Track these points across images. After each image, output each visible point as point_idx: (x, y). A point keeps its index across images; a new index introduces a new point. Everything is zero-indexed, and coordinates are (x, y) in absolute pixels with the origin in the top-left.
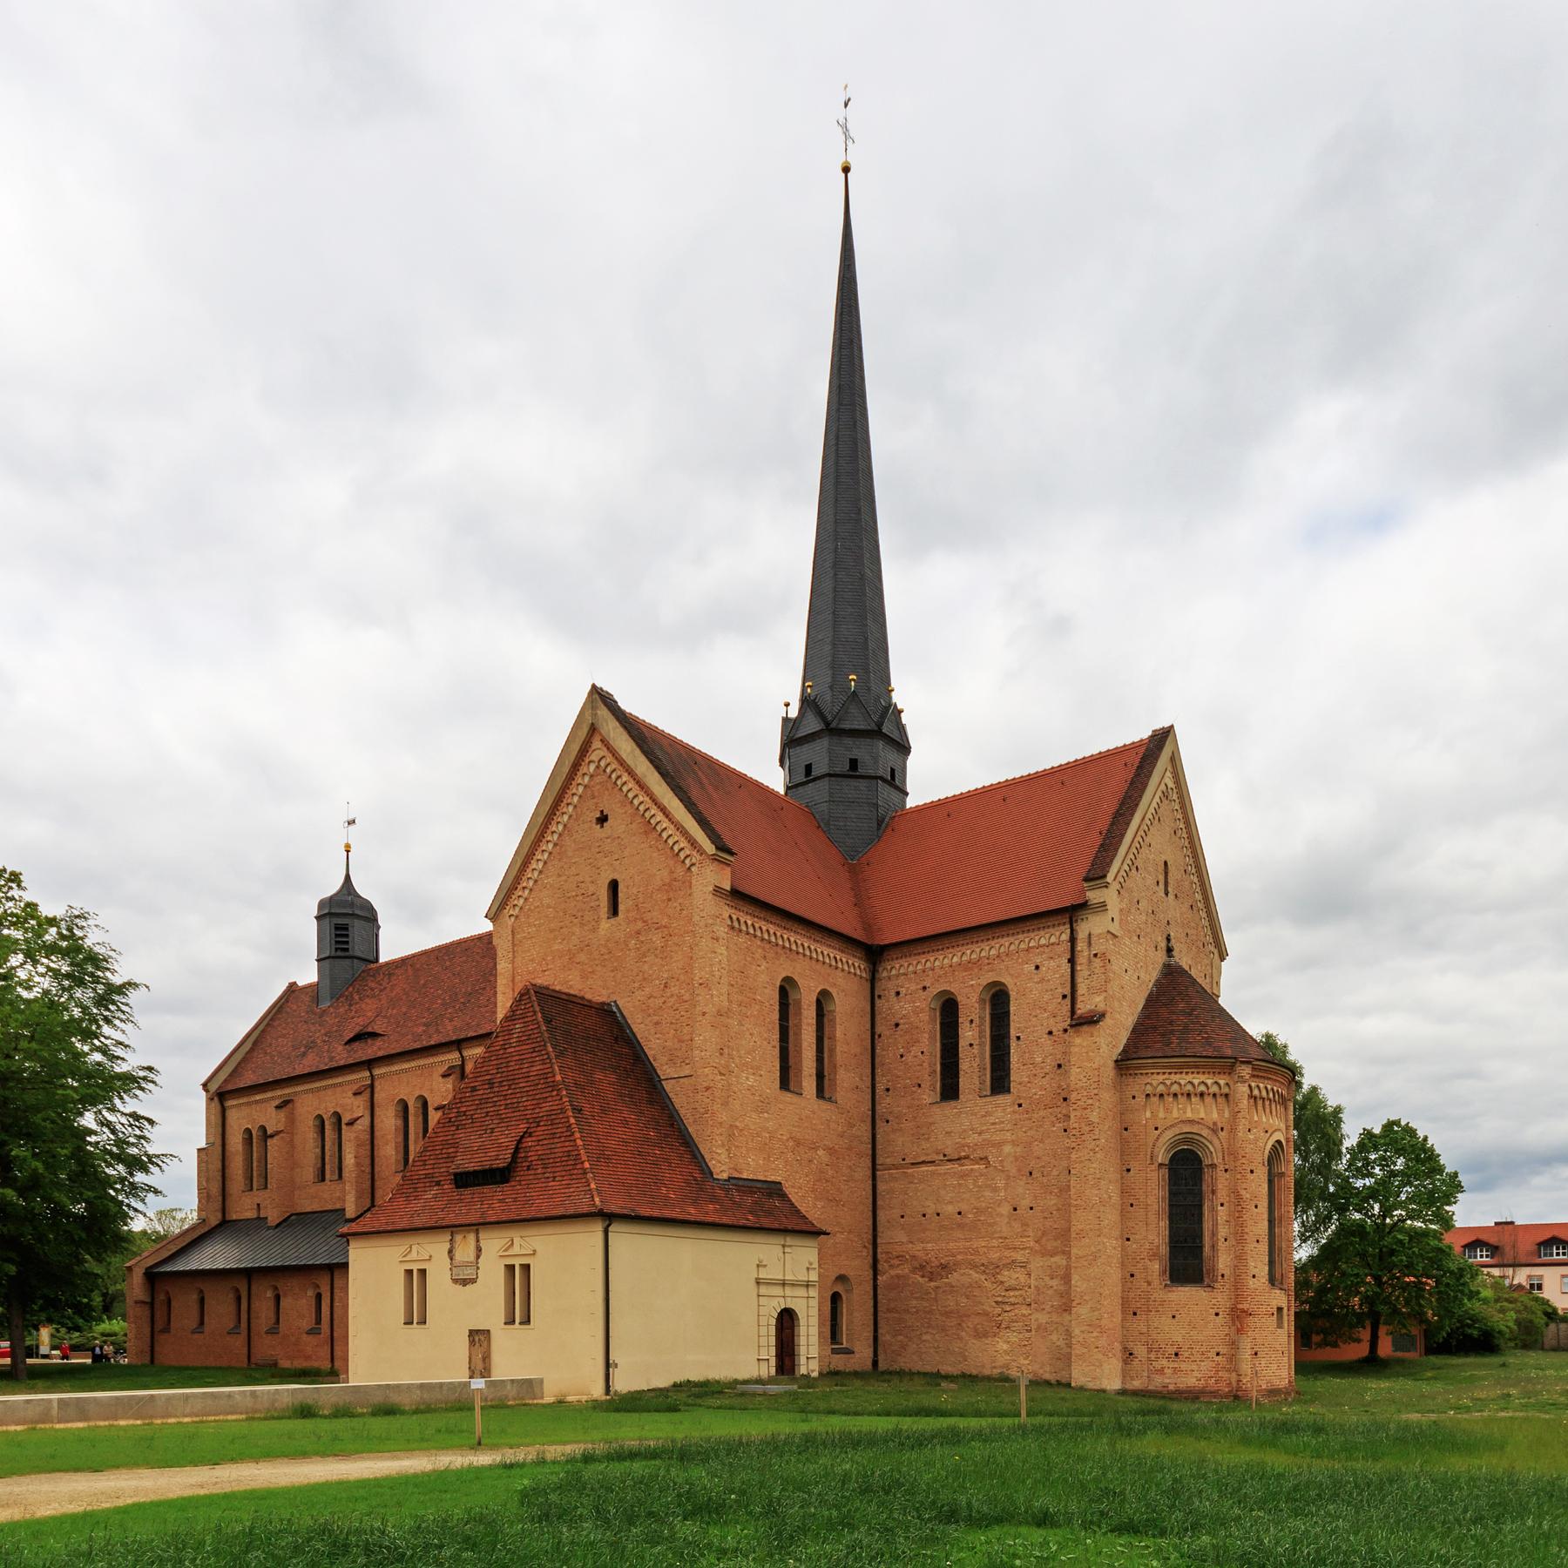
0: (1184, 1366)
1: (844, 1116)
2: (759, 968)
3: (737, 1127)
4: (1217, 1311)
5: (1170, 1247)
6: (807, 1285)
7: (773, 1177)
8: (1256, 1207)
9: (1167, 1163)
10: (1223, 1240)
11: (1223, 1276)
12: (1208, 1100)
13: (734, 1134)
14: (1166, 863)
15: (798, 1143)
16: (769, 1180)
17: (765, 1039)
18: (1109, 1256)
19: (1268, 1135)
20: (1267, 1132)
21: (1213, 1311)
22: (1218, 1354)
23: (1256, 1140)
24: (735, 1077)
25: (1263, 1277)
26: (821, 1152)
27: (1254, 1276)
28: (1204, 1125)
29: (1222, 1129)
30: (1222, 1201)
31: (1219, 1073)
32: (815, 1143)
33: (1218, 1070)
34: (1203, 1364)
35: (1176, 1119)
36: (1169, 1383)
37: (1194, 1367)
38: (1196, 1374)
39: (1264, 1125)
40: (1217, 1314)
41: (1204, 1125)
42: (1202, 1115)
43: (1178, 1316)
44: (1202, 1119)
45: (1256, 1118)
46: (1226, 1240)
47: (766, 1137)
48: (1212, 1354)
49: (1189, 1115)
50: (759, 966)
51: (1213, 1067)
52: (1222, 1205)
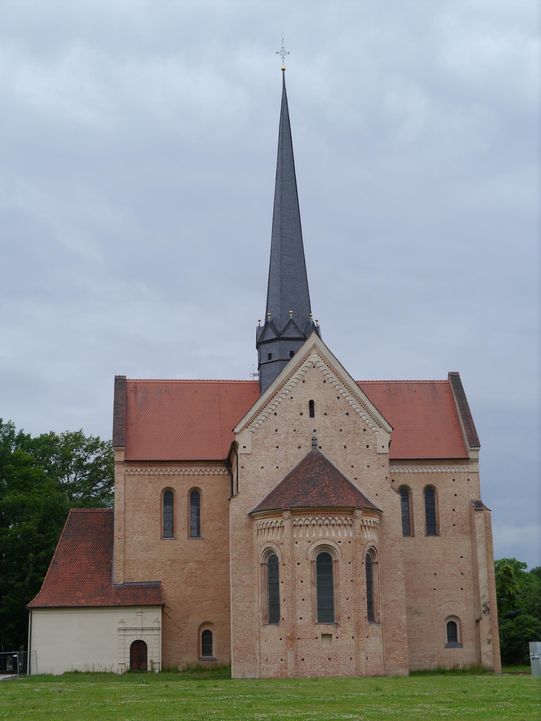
0: (269, 666)
1: (210, 544)
2: (146, 488)
3: (131, 560)
4: (281, 637)
5: (270, 605)
6: (153, 629)
7: (156, 579)
8: (302, 582)
9: (267, 562)
10: (283, 600)
11: (283, 619)
12: (275, 530)
13: (129, 563)
14: (311, 403)
15: (174, 561)
16: (152, 581)
17: (150, 518)
18: (241, 611)
19: (311, 543)
20: (310, 542)
21: (279, 638)
22: (282, 660)
23: (301, 547)
24: (130, 538)
25: (307, 618)
26: (191, 564)
27: (301, 618)
28: (274, 543)
29: (282, 544)
30: (282, 580)
31: (279, 516)
32: (187, 560)
33: (277, 515)
34: (275, 665)
35: (265, 541)
36: (265, 675)
37: (272, 667)
38: (273, 670)
39: (307, 539)
40: (281, 639)
41: (274, 543)
42: (273, 538)
43: (267, 640)
44: (273, 540)
45: (301, 536)
46: (284, 600)
47: (151, 562)
48: (279, 660)
49: (269, 538)
50: (147, 487)
51: (274, 514)
52: (282, 582)
